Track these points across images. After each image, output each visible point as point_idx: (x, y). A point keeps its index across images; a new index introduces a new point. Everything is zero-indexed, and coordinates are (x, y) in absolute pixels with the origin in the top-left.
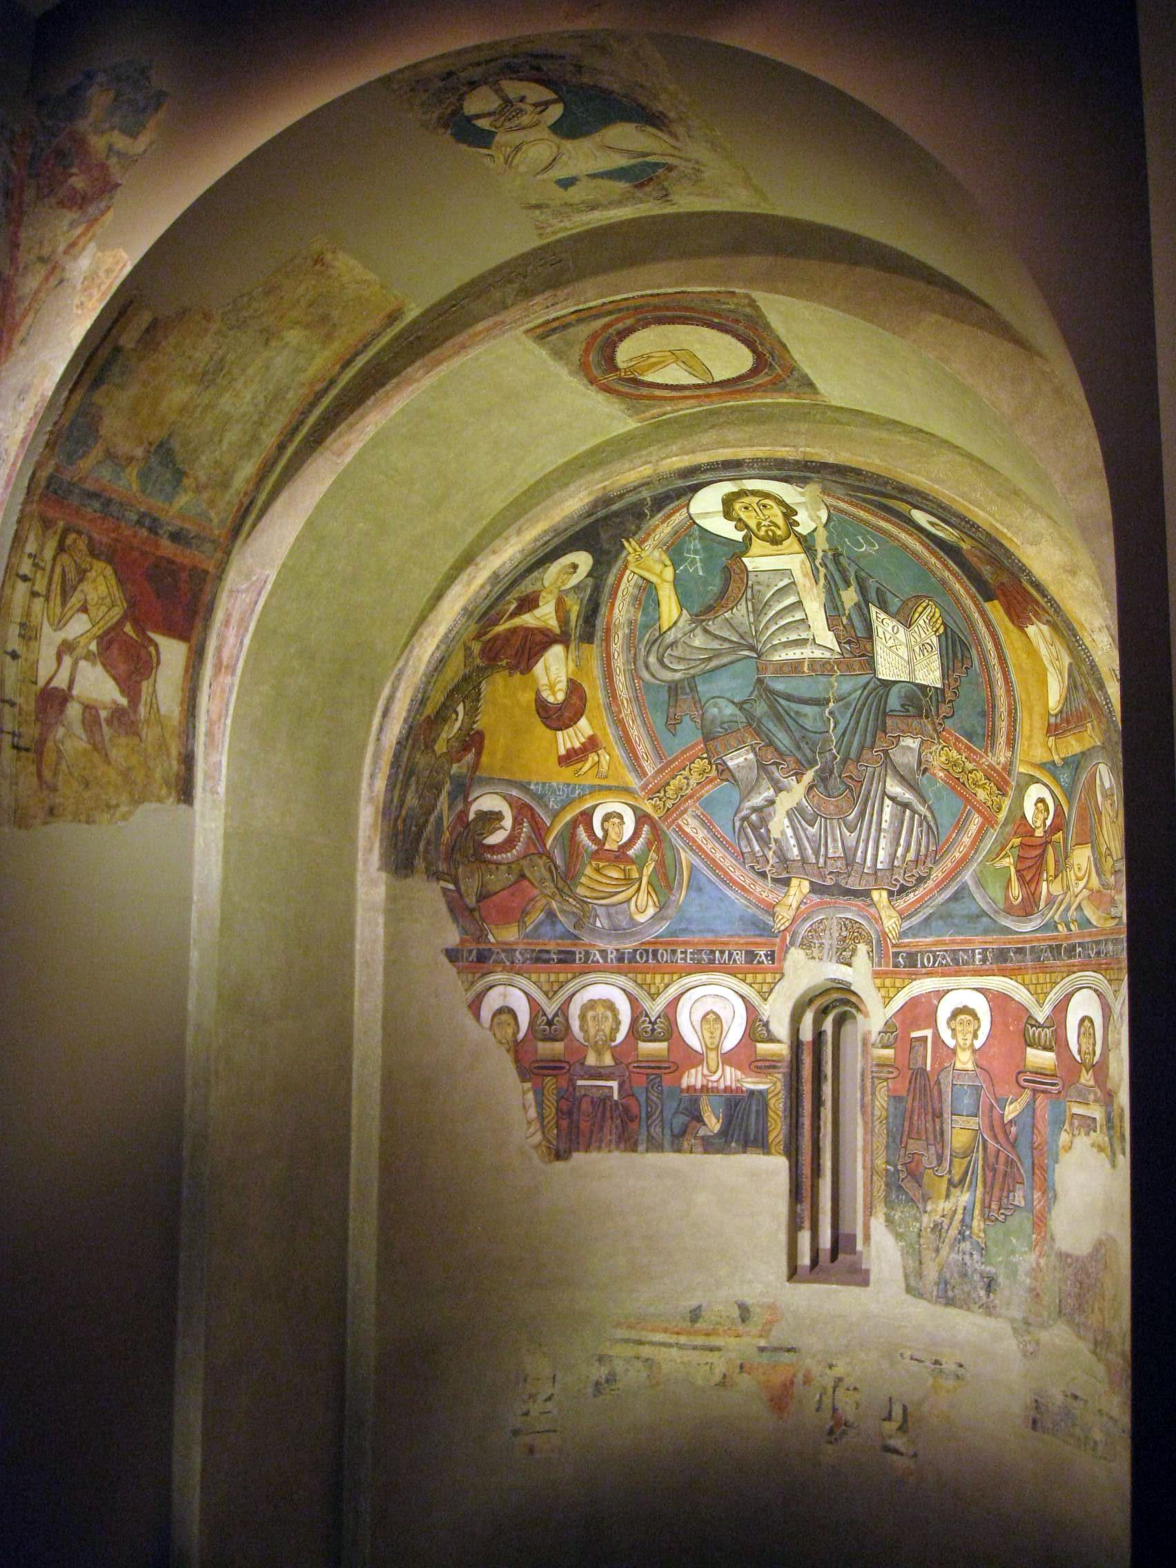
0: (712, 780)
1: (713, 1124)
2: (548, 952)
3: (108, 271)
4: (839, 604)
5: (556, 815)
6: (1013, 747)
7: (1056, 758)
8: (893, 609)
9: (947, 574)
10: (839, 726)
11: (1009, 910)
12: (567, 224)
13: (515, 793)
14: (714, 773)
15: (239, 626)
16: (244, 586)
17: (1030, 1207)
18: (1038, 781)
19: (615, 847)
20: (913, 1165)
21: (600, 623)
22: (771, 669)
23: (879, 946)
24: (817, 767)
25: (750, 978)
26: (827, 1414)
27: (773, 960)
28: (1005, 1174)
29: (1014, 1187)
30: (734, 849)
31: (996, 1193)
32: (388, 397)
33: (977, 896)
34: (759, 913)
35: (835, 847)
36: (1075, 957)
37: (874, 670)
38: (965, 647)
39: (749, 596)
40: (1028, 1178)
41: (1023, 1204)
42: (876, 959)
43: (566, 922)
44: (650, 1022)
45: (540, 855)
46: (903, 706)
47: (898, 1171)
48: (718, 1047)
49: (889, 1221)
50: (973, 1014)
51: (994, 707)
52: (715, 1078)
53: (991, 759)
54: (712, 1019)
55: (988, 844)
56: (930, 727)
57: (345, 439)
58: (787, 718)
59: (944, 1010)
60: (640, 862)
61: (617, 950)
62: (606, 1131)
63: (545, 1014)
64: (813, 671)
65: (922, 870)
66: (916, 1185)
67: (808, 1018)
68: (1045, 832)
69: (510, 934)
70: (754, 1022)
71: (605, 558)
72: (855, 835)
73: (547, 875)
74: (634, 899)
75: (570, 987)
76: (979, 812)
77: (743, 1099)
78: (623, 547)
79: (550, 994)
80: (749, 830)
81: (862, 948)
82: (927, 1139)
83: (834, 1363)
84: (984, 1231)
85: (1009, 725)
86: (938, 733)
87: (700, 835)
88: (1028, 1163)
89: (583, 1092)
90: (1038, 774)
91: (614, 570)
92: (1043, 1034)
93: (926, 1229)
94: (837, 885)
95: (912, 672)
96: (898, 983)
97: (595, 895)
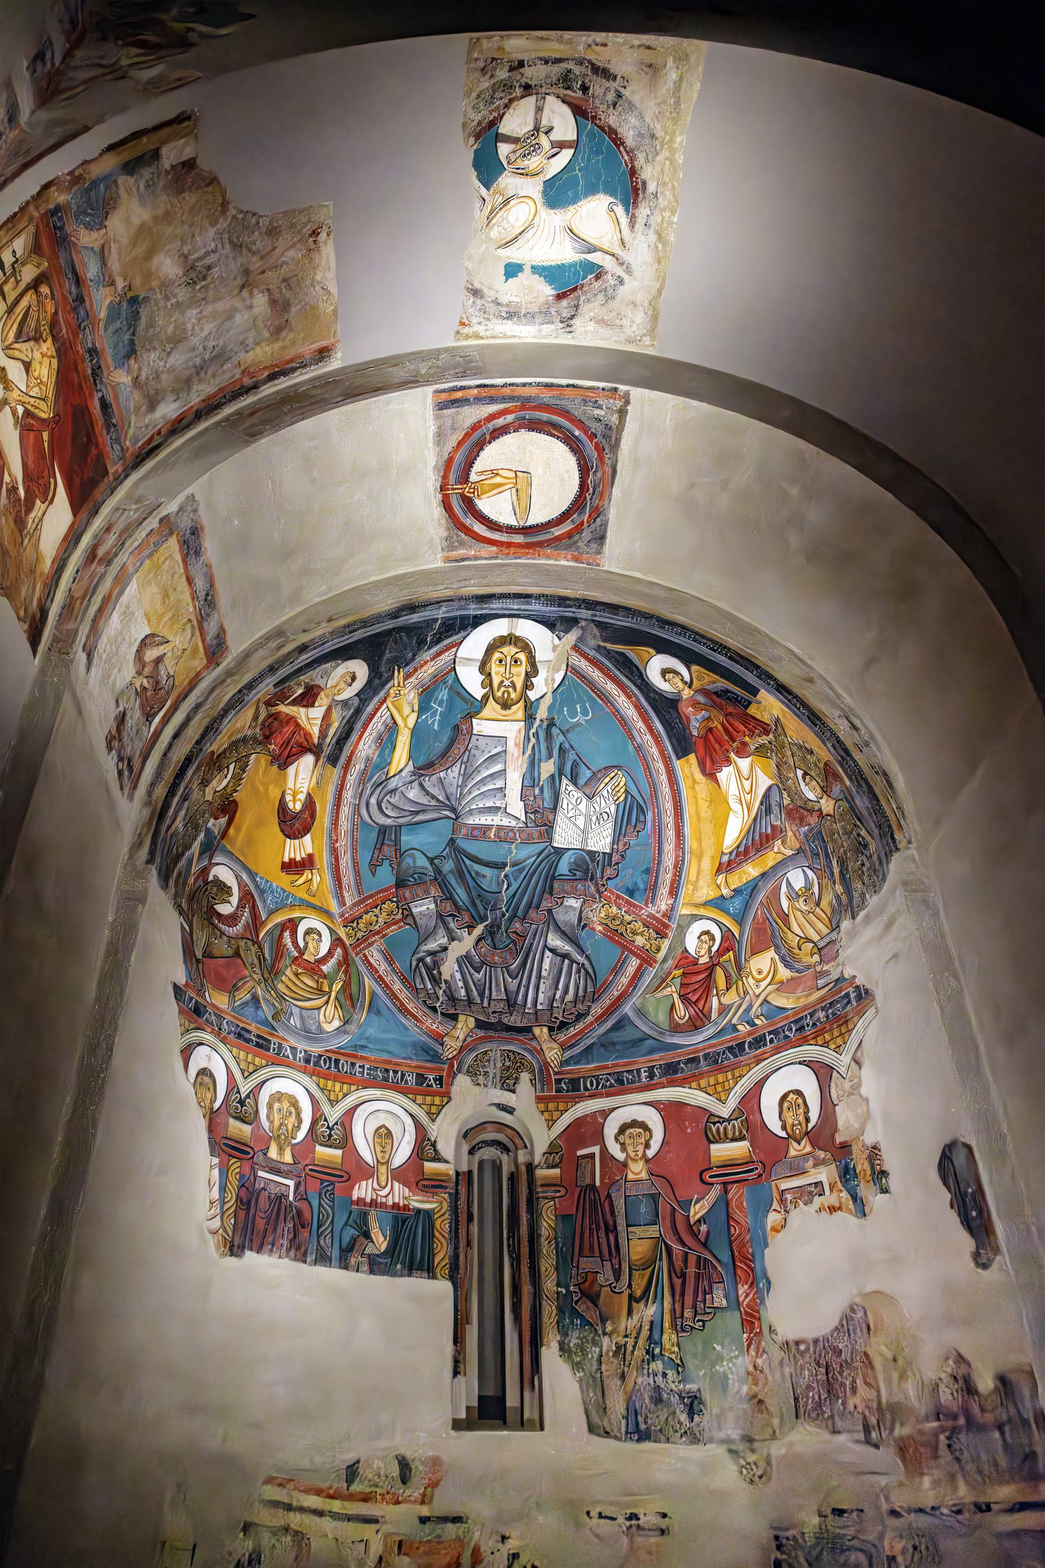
0: (398, 921)
1: (380, 1242)
2: (250, 1032)
4: (536, 774)
8: (581, 782)
10: (510, 889)
11: (676, 1029)
12: (480, 330)
14: (399, 916)
20: (587, 1284)
22: (464, 831)
23: (542, 1075)
25: (420, 1099)
30: (409, 983)
35: (498, 990)
37: (551, 839)
39: (465, 760)
42: (538, 1086)
43: (267, 1011)
44: (328, 1127)
45: (254, 943)
47: (569, 1293)
48: (387, 1162)
50: (644, 1126)
52: (384, 1193)
53: (652, 909)
55: (647, 979)
56: (593, 889)
58: (467, 875)
59: (611, 1129)
60: (331, 979)
61: (306, 1051)
63: (238, 1092)
65: (581, 1007)
66: (590, 1304)
67: (466, 1148)
69: (220, 1000)
72: (516, 982)
73: (256, 961)
74: (323, 1009)
76: (637, 956)
79: (246, 1074)
81: (525, 1077)
82: (601, 1256)
84: (678, 1345)
86: (600, 893)
87: (383, 967)
89: (262, 1185)
93: (607, 1354)
94: (500, 1022)
95: (585, 840)
96: (561, 1107)
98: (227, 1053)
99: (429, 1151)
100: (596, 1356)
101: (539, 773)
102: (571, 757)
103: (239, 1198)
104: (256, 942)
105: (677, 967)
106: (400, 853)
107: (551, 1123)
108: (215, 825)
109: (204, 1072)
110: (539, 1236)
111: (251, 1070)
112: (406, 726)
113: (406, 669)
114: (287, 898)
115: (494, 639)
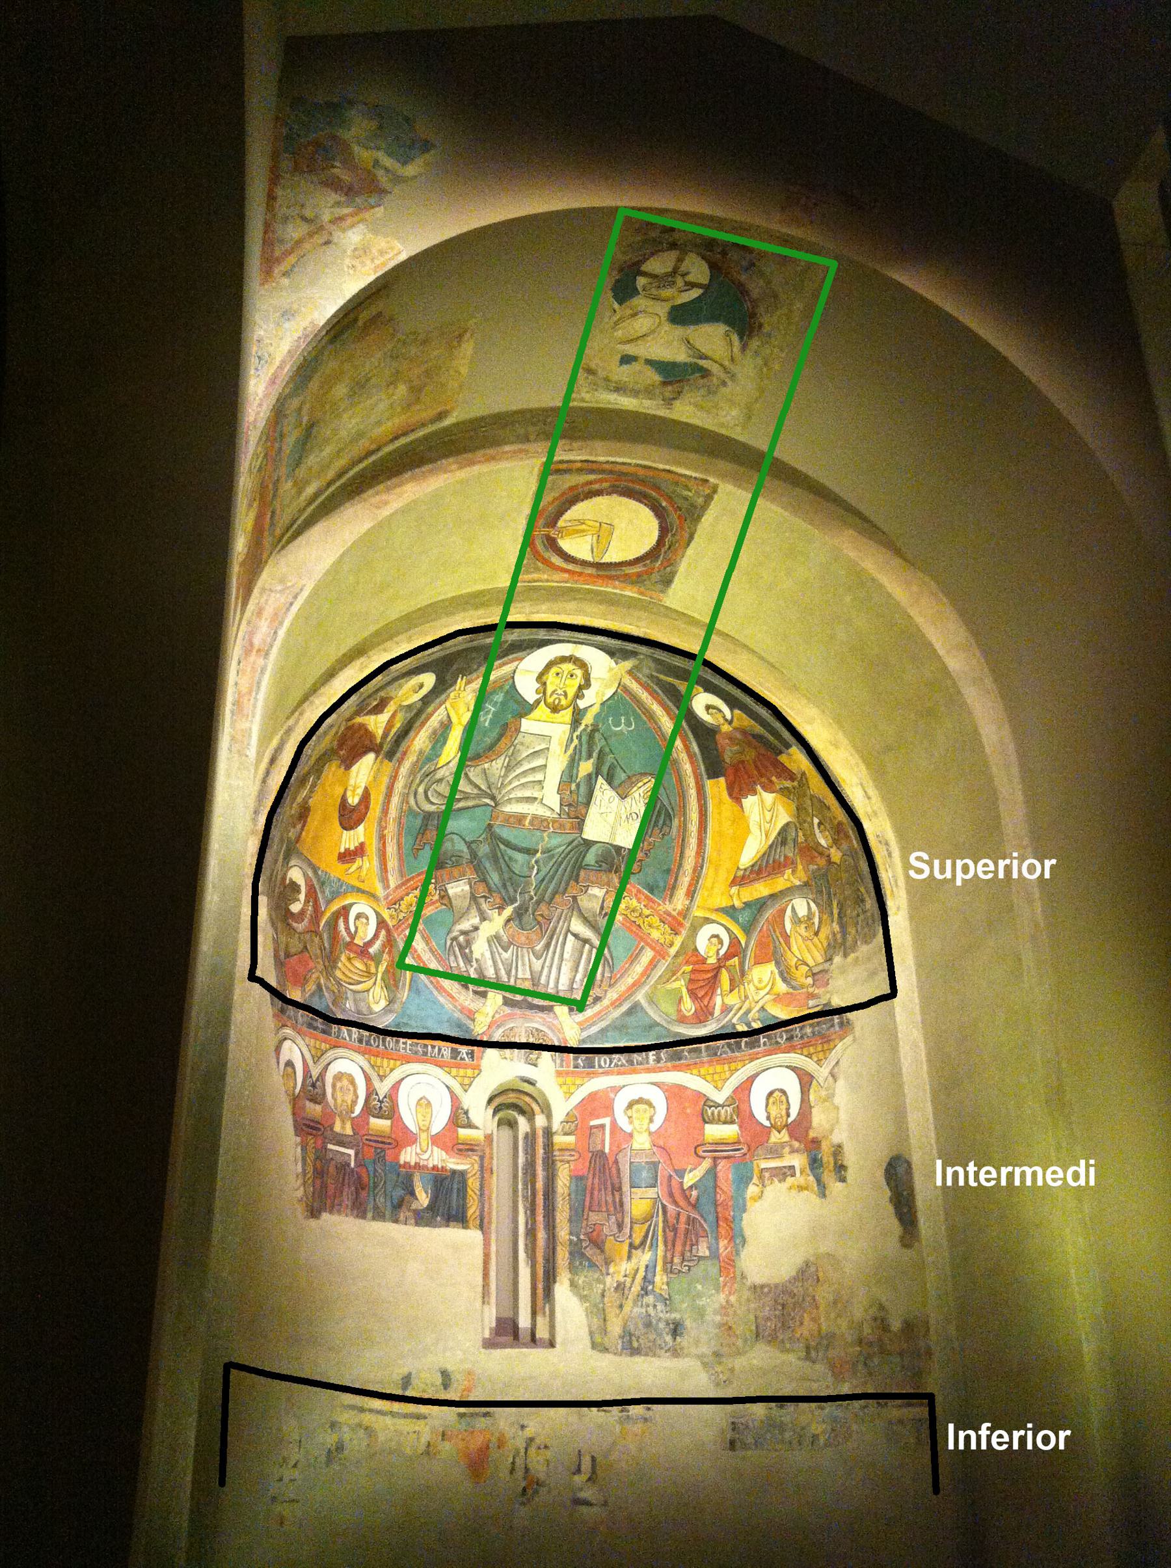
1: (423, 1199)
3: (382, 253)
4: (575, 771)
5: (329, 902)
6: (693, 897)
7: (738, 904)
8: (616, 782)
9: (683, 756)
11: (682, 1020)
12: (587, 397)
13: (310, 873)
15: (273, 621)
16: (279, 588)
17: (715, 1255)
18: (713, 921)
19: (361, 944)
20: (595, 1234)
21: (401, 749)
24: (516, 905)
25: (454, 1071)
26: (520, 1474)
27: (472, 1057)
28: (687, 1230)
29: (697, 1242)
31: (679, 1248)
32: (424, 476)
33: (651, 1013)
34: (461, 1016)
35: (524, 970)
36: (759, 1046)
38: (669, 817)
40: (712, 1232)
41: (707, 1253)
44: (379, 1101)
46: (596, 862)
47: (581, 1241)
49: (573, 1284)
50: (649, 1104)
51: (680, 865)
52: (425, 1156)
53: (669, 907)
54: (424, 1103)
57: (384, 497)
58: (501, 861)
59: (620, 1103)
60: (377, 959)
62: (345, 1194)
63: (311, 1077)
64: (532, 825)
67: (490, 1111)
68: (719, 960)
70: (458, 1108)
71: (442, 686)
72: (541, 961)
73: (318, 951)
74: (372, 991)
75: (330, 1054)
76: (653, 948)
77: (446, 1178)
78: (455, 682)
80: (457, 949)
82: (608, 1210)
83: (525, 1423)
84: (668, 1284)
85: (692, 879)
88: (711, 1218)
90: (713, 916)
91: (438, 701)
92: (723, 1112)
93: (609, 1289)
95: (613, 834)
96: (578, 1081)
97: (347, 980)
98: (302, 1042)
99: (463, 1117)
100: (600, 1291)
101: (578, 771)
102: (610, 759)
103: (315, 1169)
104: (317, 933)
105: (687, 963)
107: (569, 1094)
109: (289, 1064)
110: (554, 1192)
111: (319, 1055)
112: (460, 723)
113: (469, 677)
114: (341, 886)
115: (556, 658)
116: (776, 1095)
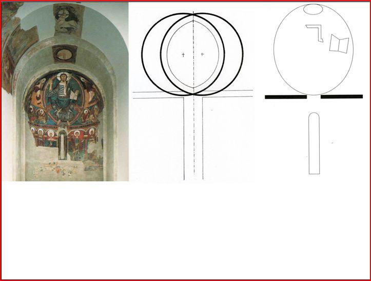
1: (51, 144)
54: (51, 133)
69: (33, 122)
71: (47, 80)
87: (50, 114)
106: (51, 100)
108: (29, 102)
116: (92, 132)
